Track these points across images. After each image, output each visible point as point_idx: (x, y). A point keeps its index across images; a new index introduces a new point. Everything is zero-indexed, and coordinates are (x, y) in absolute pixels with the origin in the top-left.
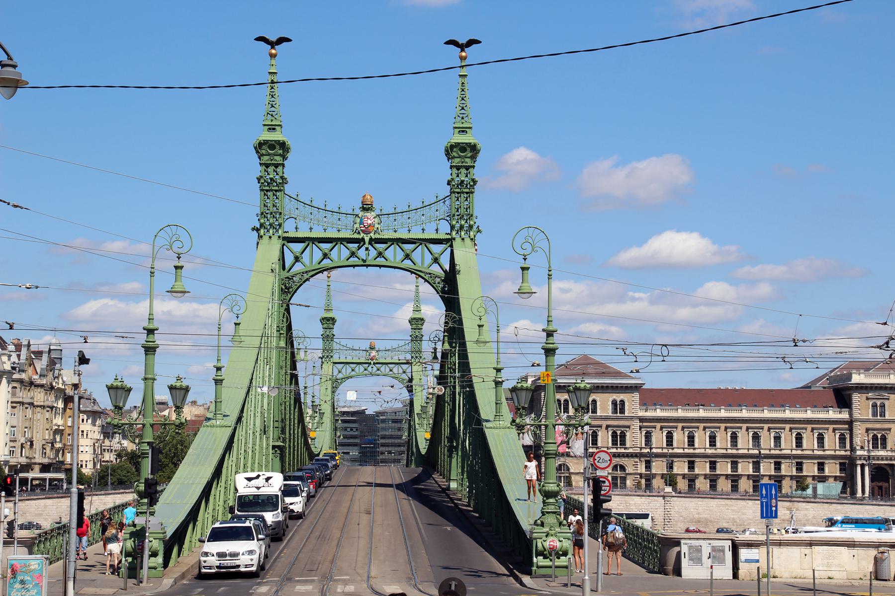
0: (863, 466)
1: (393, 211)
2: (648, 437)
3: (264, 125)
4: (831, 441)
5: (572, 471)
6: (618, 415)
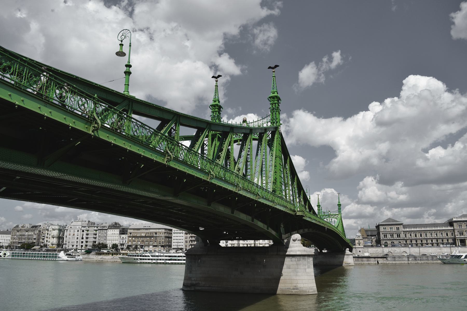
0: (458, 240)
1: (253, 121)
2: (406, 235)
3: (213, 101)
4: (450, 234)
5: (388, 243)
6: (398, 230)
